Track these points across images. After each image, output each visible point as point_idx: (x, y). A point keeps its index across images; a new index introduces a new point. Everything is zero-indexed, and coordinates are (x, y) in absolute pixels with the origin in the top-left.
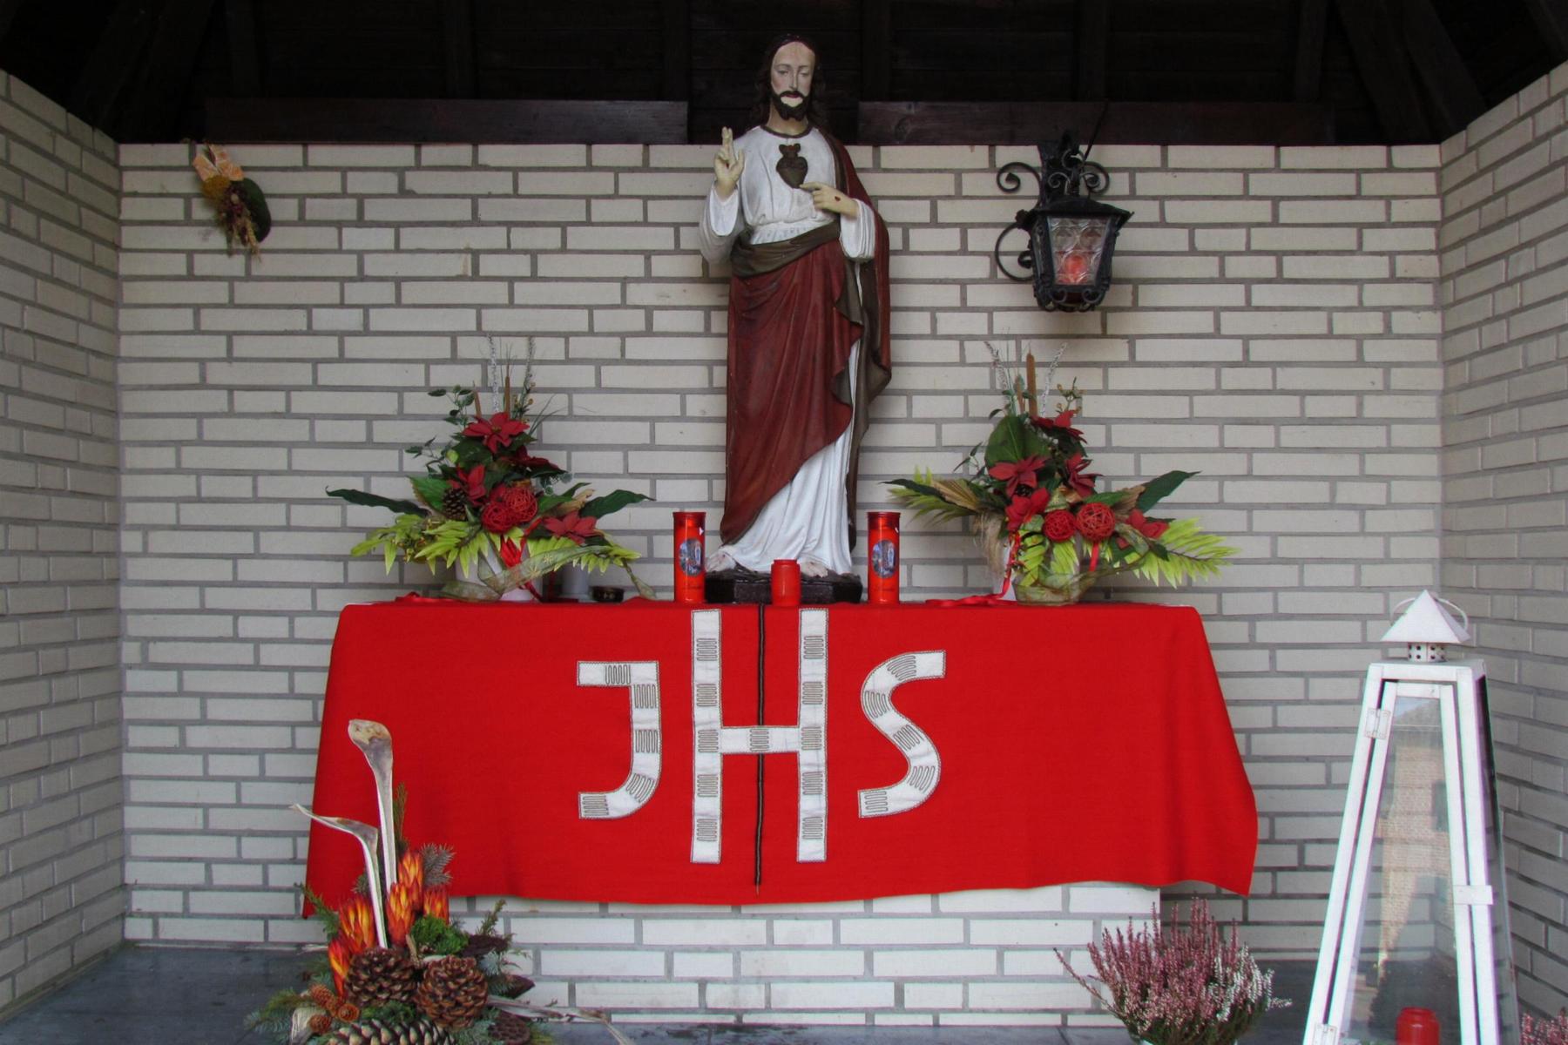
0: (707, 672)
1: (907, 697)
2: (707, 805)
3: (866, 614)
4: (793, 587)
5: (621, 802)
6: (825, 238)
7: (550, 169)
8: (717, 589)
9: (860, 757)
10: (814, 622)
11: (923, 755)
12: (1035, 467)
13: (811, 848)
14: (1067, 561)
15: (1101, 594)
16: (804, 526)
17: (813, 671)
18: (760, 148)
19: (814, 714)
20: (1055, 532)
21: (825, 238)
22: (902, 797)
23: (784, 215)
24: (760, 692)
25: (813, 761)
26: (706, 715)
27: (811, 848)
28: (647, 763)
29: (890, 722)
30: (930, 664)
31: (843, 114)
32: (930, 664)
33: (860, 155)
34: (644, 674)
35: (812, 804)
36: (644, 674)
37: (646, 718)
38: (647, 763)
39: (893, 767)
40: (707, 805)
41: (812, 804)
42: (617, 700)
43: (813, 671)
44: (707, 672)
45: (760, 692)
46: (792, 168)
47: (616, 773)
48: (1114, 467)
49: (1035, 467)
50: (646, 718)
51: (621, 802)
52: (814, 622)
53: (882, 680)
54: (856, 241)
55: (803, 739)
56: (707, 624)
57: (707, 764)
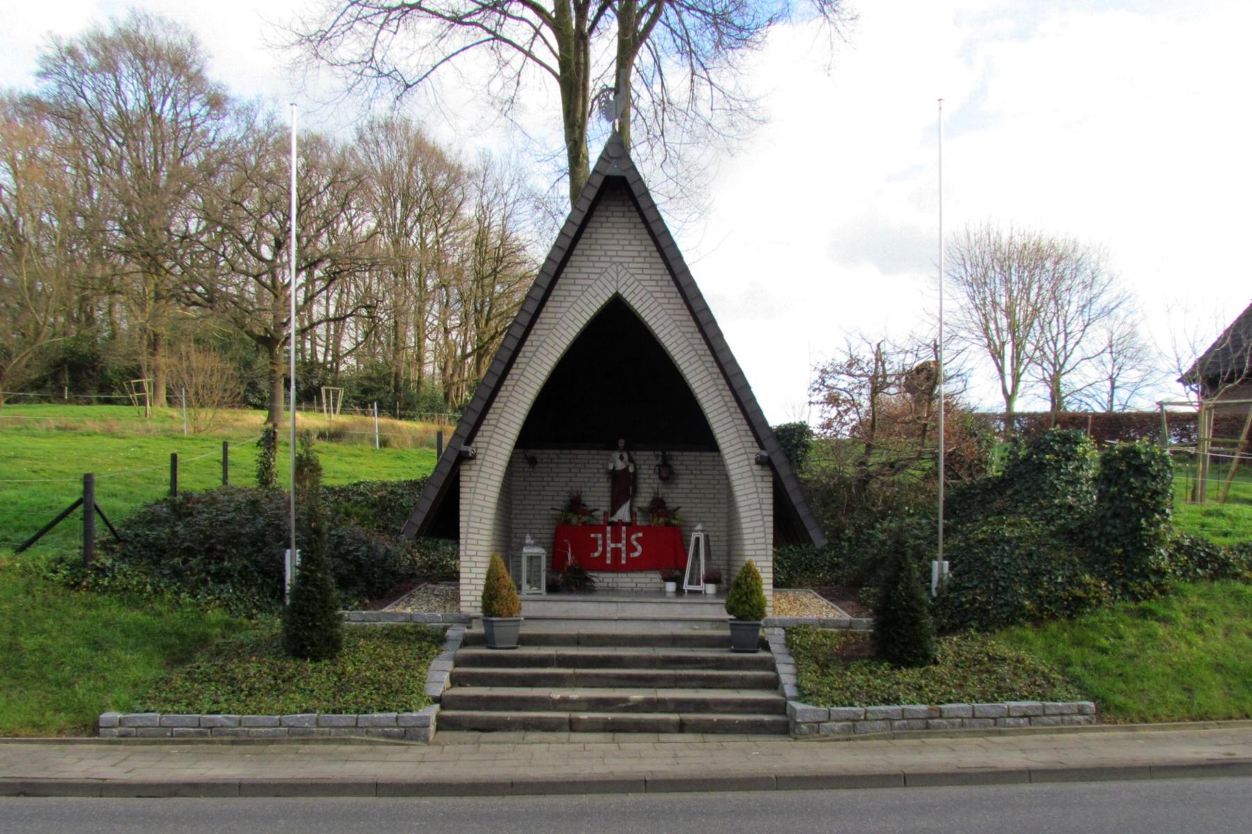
0: (609, 535)
1: (638, 539)
2: (609, 555)
3: (632, 527)
4: (621, 523)
5: (596, 554)
6: (627, 469)
7: (583, 454)
8: (611, 524)
9: (631, 548)
10: (624, 528)
11: (639, 548)
12: (658, 505)
13: (624, 562)
14: (661, 520)
15: (668, 524)
16: (623, 514)
17: (624, 535)
18: (616, 455)
19: (624, 542)
20: (659, 516)
21: (626, 469)
22: (637, 554)
23: (620, 465)
24: (616, 539)
25: (624, 549)
26: (609, 542)
27: (624, 562)
28: (600, 549)
29: (635, 543)
30: (640, 535)
31: (628, 448)
32: (640, 535)
33: (632, 453)
34: (600, 536)
35: (624, 555)
36: (600, 536)
37: (600, 542)
38: (600, 549)
39: (635, 550)
40: (609, 555)
41: (624, 555)
42: (596, 540)
43: (624, 535)
44: (609, 535)
45: (616, 539)
46: (621, 458)
47: (596, 550)
48: (671, 505)
49: (658, 505)
50: (600, 542)
51: (596, 554)
52: (624, 528)
53: (633, 537)
54: (631, 469)
55: (622, 545)
56: (609, 528)
57: (609, 549)
